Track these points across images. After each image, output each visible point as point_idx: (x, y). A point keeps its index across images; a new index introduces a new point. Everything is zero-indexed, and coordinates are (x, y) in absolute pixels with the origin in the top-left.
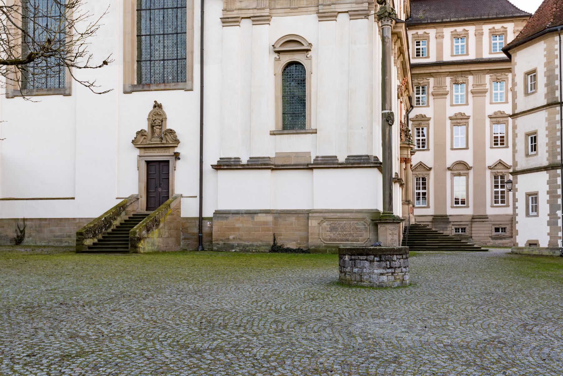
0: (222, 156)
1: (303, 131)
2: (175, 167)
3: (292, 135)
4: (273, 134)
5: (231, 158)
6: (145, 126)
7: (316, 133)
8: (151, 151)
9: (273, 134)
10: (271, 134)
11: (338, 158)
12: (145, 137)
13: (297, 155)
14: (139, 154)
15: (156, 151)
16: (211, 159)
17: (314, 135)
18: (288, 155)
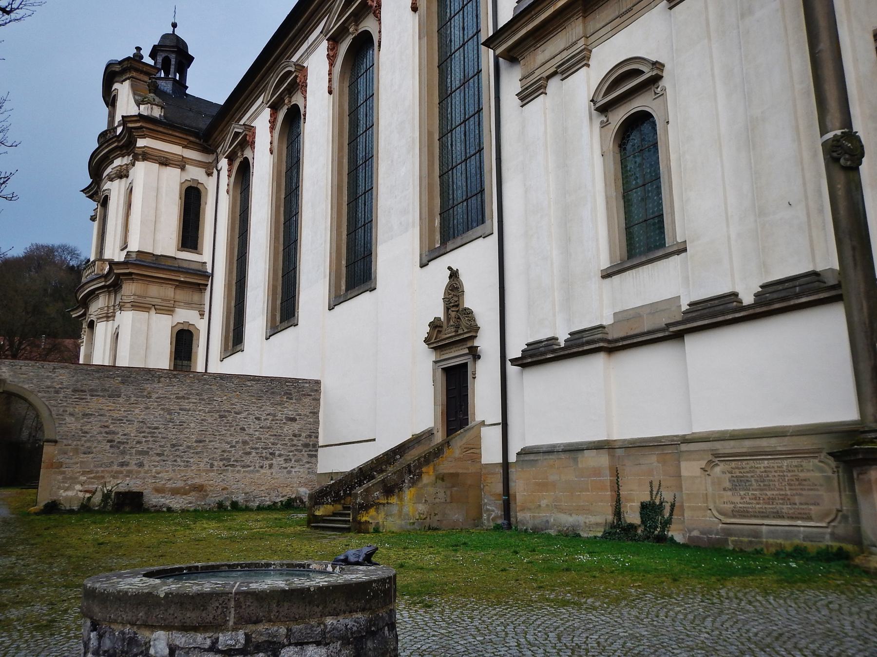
0: (531, 340)
1: (660, 253)
2: (474, 374)
3: (640, 269)
4: (607, 275)
5: (540, 342)
6: (440, 313)
7: (685, 250)
8: (447, 351)
9: (607, 275)
10: (603, 277)
11: (740, 296)
12: (440, 329)
13: (654, 308)
14: (434, 360)
15: (452, 350)
16: (515, 351)
17: (683, 254)
18: (635, 314)
